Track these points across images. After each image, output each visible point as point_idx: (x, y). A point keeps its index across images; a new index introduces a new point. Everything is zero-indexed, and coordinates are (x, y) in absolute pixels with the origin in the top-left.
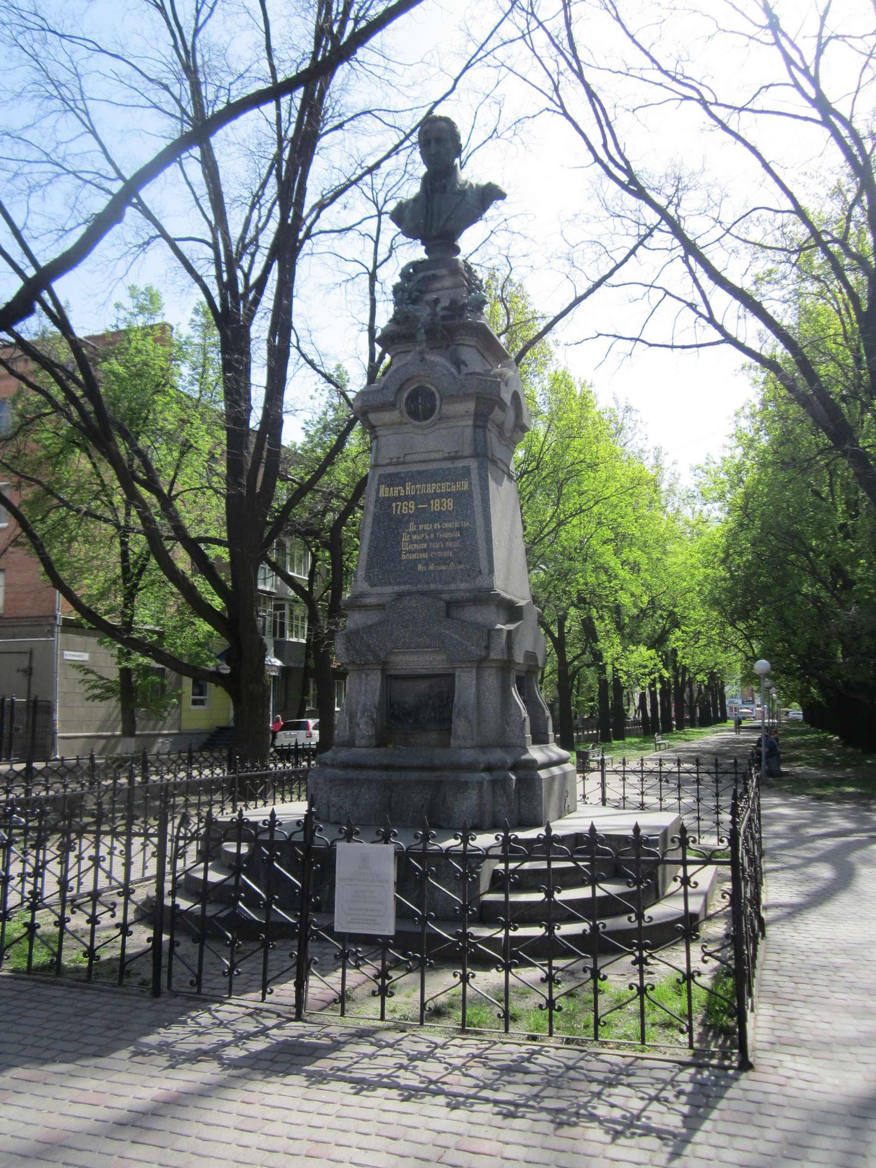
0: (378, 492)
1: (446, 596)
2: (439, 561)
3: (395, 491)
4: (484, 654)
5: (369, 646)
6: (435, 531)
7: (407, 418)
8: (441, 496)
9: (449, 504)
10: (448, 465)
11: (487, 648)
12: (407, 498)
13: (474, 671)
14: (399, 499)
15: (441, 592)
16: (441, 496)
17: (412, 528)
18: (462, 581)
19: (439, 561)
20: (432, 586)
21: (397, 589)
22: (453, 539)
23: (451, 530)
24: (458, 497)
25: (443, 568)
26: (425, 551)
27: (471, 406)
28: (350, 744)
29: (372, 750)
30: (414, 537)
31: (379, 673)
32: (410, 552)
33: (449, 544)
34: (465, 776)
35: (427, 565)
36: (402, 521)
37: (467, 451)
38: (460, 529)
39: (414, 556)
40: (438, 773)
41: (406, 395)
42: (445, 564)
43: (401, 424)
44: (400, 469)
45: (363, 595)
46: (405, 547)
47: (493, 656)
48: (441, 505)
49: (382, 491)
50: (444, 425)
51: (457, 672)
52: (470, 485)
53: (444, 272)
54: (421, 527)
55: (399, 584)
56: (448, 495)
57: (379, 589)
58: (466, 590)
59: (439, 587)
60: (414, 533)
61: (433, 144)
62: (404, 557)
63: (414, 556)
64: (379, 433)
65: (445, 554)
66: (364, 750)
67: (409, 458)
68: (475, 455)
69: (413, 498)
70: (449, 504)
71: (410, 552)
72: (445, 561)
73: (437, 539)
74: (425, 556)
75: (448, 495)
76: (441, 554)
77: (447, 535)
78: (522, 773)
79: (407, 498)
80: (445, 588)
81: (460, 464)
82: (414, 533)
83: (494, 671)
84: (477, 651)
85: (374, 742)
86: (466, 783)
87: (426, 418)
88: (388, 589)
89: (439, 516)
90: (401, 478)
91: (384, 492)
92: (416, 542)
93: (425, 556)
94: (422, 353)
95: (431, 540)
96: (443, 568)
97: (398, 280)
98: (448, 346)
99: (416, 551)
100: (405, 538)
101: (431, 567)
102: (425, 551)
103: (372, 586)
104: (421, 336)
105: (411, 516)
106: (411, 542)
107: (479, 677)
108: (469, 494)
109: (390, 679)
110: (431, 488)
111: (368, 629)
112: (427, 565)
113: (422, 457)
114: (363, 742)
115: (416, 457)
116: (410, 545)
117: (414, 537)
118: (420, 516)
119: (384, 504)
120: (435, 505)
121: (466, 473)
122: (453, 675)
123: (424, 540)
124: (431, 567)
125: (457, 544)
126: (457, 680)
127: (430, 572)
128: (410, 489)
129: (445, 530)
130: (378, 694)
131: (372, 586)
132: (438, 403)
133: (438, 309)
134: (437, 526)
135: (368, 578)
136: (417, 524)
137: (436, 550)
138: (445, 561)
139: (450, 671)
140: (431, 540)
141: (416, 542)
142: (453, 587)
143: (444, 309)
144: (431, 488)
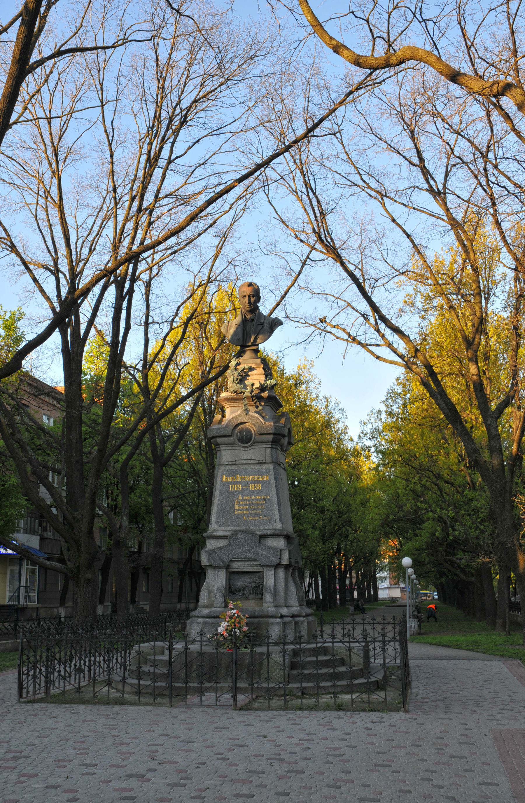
0: (222, 479)
1: (258, 533)
3: (231, 479)
4: (278, 561)
6: (252, 500)
7: (237, 441)
10: (257, 466)
12: (237, 483)
13: (273, 569)
14: (233, 483)
15: (255, 530)
17: (240, 498)
20: (251, 528)
21: (232, 528)
22: (261, 505)
23: (260, 500)
24: (263, 483)
25: (256, 518)
26: (247, 509)
27: (271, 437)
29: (223, 609)
30: (241, 503)
31: (225, 570)
32: (240, 510)
34: (271, 620)
35: (248, 517)
36: (234, 493)
37: (268, 460)
39: (241, 512)
40: (257, 619)
43: (234, 444)
44: (233, 467)
45: (215, 531)
46: (237, 507)
48: (255, 487)
49: (224, 478)
51: (265, 570)
54: (245, 498)
55: (234, 526)
56: (258, 482)
57: (224, 528)
59: (255, 528)
60: (241, 500)
62: (236, 513)
63: (241, 512)
65: (257, 512)
66: (219, 609)
67: (238, 462)
68: (272, 462)
69: (240, 483)
70: (260, 486)
71: (240, 510)
73: (253, 504)
74: (247, 512)
75: (258, 482)
76: (255, 511)
77: (258, 502)
79: (237, 483)
80: (258, 528)
81: (264, 467)
82: (241, 500)
85: (223, 605)
86: (272, 623)
87: (247, 443)
88: (229, 529)
90: (234, 472)
91: (224, 478)
96: (256, 518)
100: (237, 503)
101: (250, 518)
102: (247, 509)
103: (219, 527)
105: (239, 492)
106: (240, 505)
107: (275, 572)
110: (250, 478)
111: (220, 548)
112: (248, 517)
113: (245, 462)
114: (218, 605)
115: (241, 462)
116: (240, 505)
117: (241, 503)
118: (245, 491)
119: (226, 485)
120: (252, 487)
121: (267, 472)
123: (246, 505)
124: (250, 518)
125: (263, 507)
128: (238, 478)
129: (257, 500)
130: (224, 581)
134: (253, 497)
135: (217, 523)
136: (243, 496)
138: (258, 515)
139: (261, 570)
141: (242, 505)
144: (250, 478)
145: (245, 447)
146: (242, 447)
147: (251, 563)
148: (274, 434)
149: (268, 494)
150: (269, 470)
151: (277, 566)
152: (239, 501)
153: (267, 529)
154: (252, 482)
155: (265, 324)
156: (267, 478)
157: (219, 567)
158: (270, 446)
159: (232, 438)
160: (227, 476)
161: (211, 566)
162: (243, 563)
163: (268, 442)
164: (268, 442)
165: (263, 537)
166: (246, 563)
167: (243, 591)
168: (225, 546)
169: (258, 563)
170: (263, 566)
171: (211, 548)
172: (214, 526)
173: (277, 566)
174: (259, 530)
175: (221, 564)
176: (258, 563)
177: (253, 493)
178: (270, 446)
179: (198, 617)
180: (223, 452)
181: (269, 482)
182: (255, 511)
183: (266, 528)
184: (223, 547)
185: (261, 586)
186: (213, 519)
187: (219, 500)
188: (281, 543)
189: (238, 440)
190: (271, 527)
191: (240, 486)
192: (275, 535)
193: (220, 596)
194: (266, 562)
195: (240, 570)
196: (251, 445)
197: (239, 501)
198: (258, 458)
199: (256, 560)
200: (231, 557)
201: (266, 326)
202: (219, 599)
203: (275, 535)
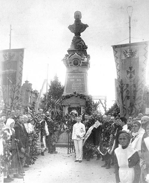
9: (80, 80)
22: (81, 86)
33: (80, 87)
35: (76, 90)
41: (73, 61)
56: (80, 78)
73: (78, 86)
74: (76, 88)
75: (80, 78)
76: (79, 88)
89: (78, 82)
97: (72, 41)
99: (74, 87)
106: (74, 86)
120: (78, 80)
123: (76, 86)
129: (80, 84)
137: (78, 87)
141: (74, 86)
157: (66, 106)
182: (79, 88)
196: (78, 66)
199: (79, 104)
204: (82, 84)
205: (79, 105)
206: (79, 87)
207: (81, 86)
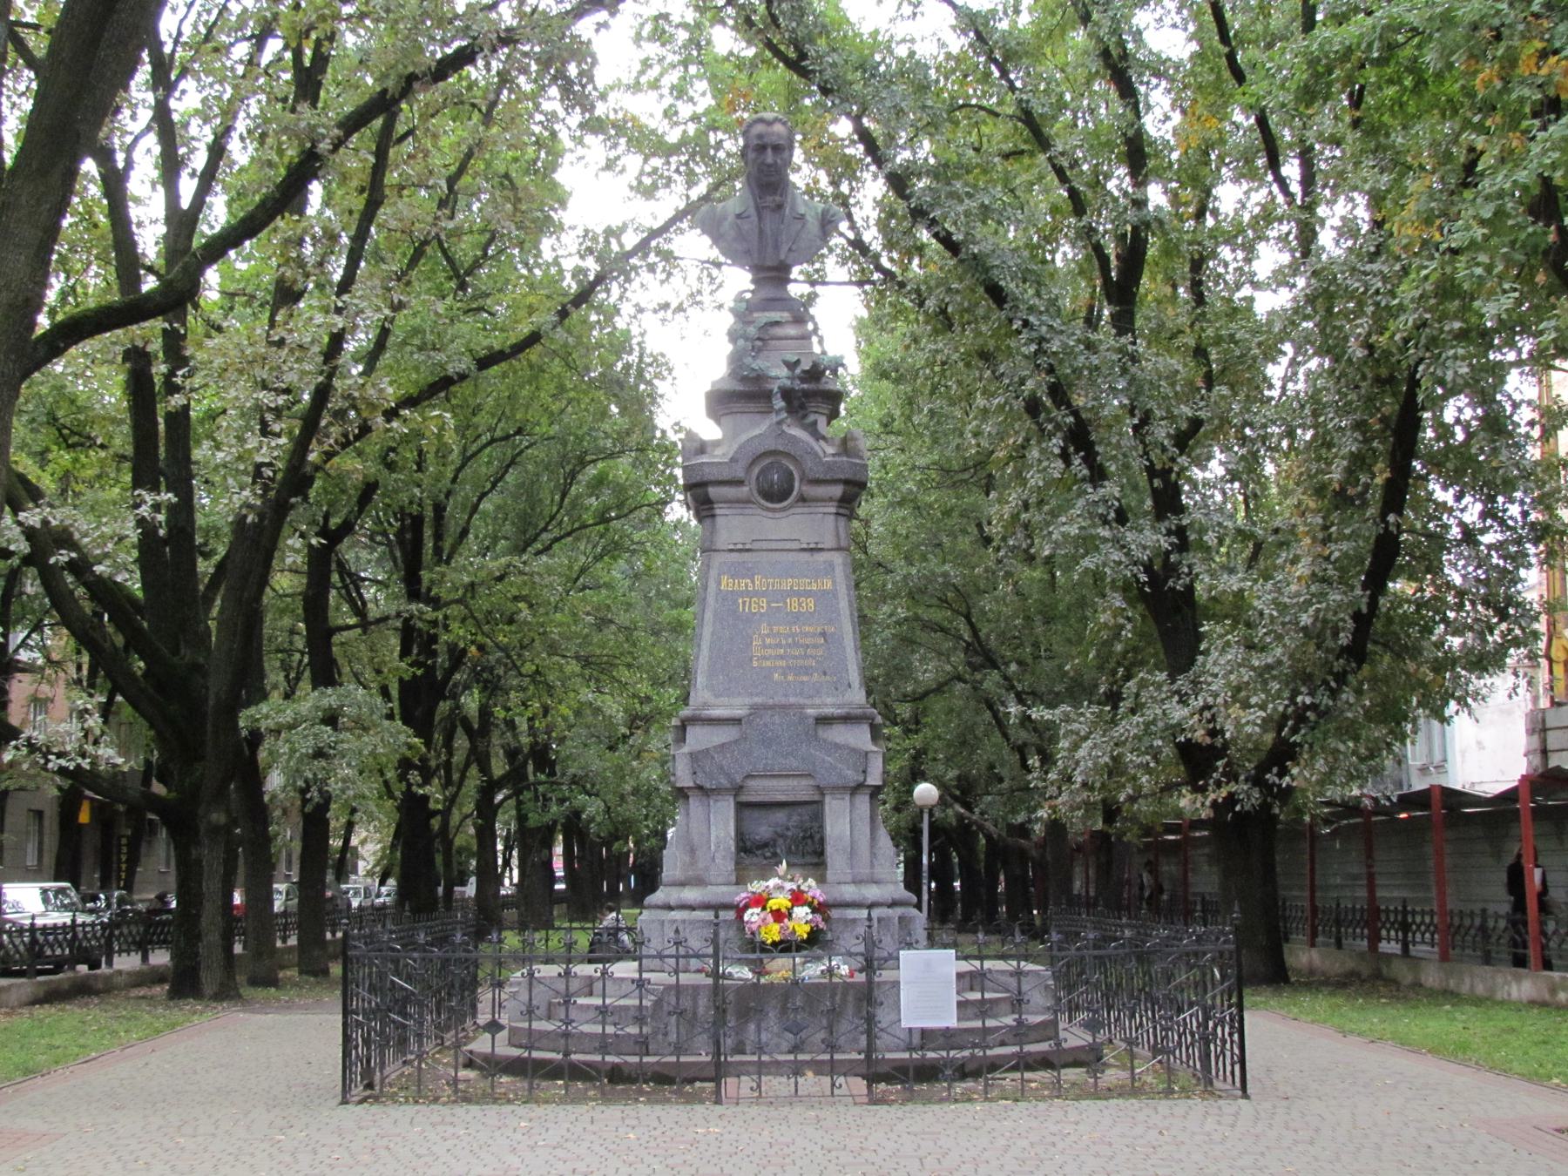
0: (719, 584)
2: (800, 670)
3: (744, 583)
4: (861, 779)
5: (722, 768)
6: (793, 635)
8: (799, 594)
10: (806, 556)
11: (864, 772)
12: (756, 594)
13: (847, 798)
15: (802, 707)
16: (799, 594)
18: (828, 695)
19: (800, 670)
20: (792, 700)
21: (748, 701)
22: (815, 646)
23: (814, 635)
24: (821, 596)
25: (805, 679)
26: (782, 657)
27: (837, 491)
28: (699, 882)
29: (733, 888)
30: (768, 641)
31: (731, 799)
32: (765, 658)
35: (785, 675)
37: (829, 542)
38: (823, 634)
39: (769, 663)
41: (756, 470)
42: (807, 674)
43: (748, 501)
45: (706, 706)
47: (870, 782)
49: (724, 582)
50: (799, 510)
51: (828, 799)
52: (834, 583)
53: (786, 316)
55: (751, 695)
56: (808, 594)
57: (725, 700)
58: (833, 705)
59: (802, 701)
60: (768, 636)
61: (769, 151)
62: (755, 664)
63: (769, 663)
64: (718, 512)
66: (725, 889)
67: (756, 546)
68: (839, 549)
71: (765, 658)
72: (807, 671)
73: (796, 645)
74: (783, 663)
75: (808, 594)
76: (800, 662)
77: (808, 641)
78: (899, 911)
79: (756, 594)
81: (821, 557)
82: (768, 636)
83: (867, 798)
84: (852, 776)
85: (733, 878)
86: (854, 921)
87: (781, 500)
88: (738, 701)
92: (770, 646)
93: (783, 663)
94: (779, 423)
95: (789, 646)
96: (805, 679)
98: (805, 416)
101: (790, 678)
102: (782, 657)
104: (779, 403)
105: (762, 615)
106: (765, 646)
108: (834, 593)
109: (742, 807)
110: (787, 584)
113: (774, 546)
114: (720, 880)
115: (765, 545)
117: (768, 641)
119: (728, 598)
120: (793, 604)
122: (820, 803)
123: (779, 645)
124: (790, 678)
126: (827, 808)
127: (789, 683)
129: (806, 635)
131: (717, 696)
132: (797, 484)
133: (798, 371)
137: (796, 657)
138: (807, 671)
139: (816, 798)
140: (789, 646)
141: (770, 646)
142: (817, 701)
143: (804, 372)
144: (787, 584)
145: (774, 510)
146: (768, 509)
147: (793, 782)
148: (847, 482)
149: (831, 622)
150: (831, 565)
151: (856, 789)
152: (763, 637)
153: (830, 704)
154: (792, 593)
155: (808, 217)
156: (828, 585)
158: (833, 510)
159: (746, 489)
160: (732, 577)
161: (700, 788)
162: (774, 783)
163: (831, 499)
164: (831, 499)
165: (824, 721)
166: (783, 783)
167: (775, 846)
168: (736, 742)
169: (812, 782)
170: (820, 790)
171: (699, 748)
172: (701, 694)
173: (856, 789)
174: (812, 706)
175: (724, 782)
176: (812, 782)
177: (797, 618)
178: (833, 510)
179: (670, 908)
180: (719, 520)
181: (834, 593)
183: (829, 700)
184: (730, 743)
185: (817, 837)
186: (700, 679)
187: (713, 634)
188: (860, 737)
189: (760, 493)
190: (840, 700)
191: (764, 602)
192: (847, 719)
193: (724, 858)
194: (834, 779)
195: (766, 799)
196: (791, 507)
197: (763, 637)
198: (807, 539)
200: (748, 769)
201: (813, 225)
202: (725, 864)
203: (847, 719)
204: (823, 634)
205: (804, 782)
206: (806, 656)
207: (815, 646)
